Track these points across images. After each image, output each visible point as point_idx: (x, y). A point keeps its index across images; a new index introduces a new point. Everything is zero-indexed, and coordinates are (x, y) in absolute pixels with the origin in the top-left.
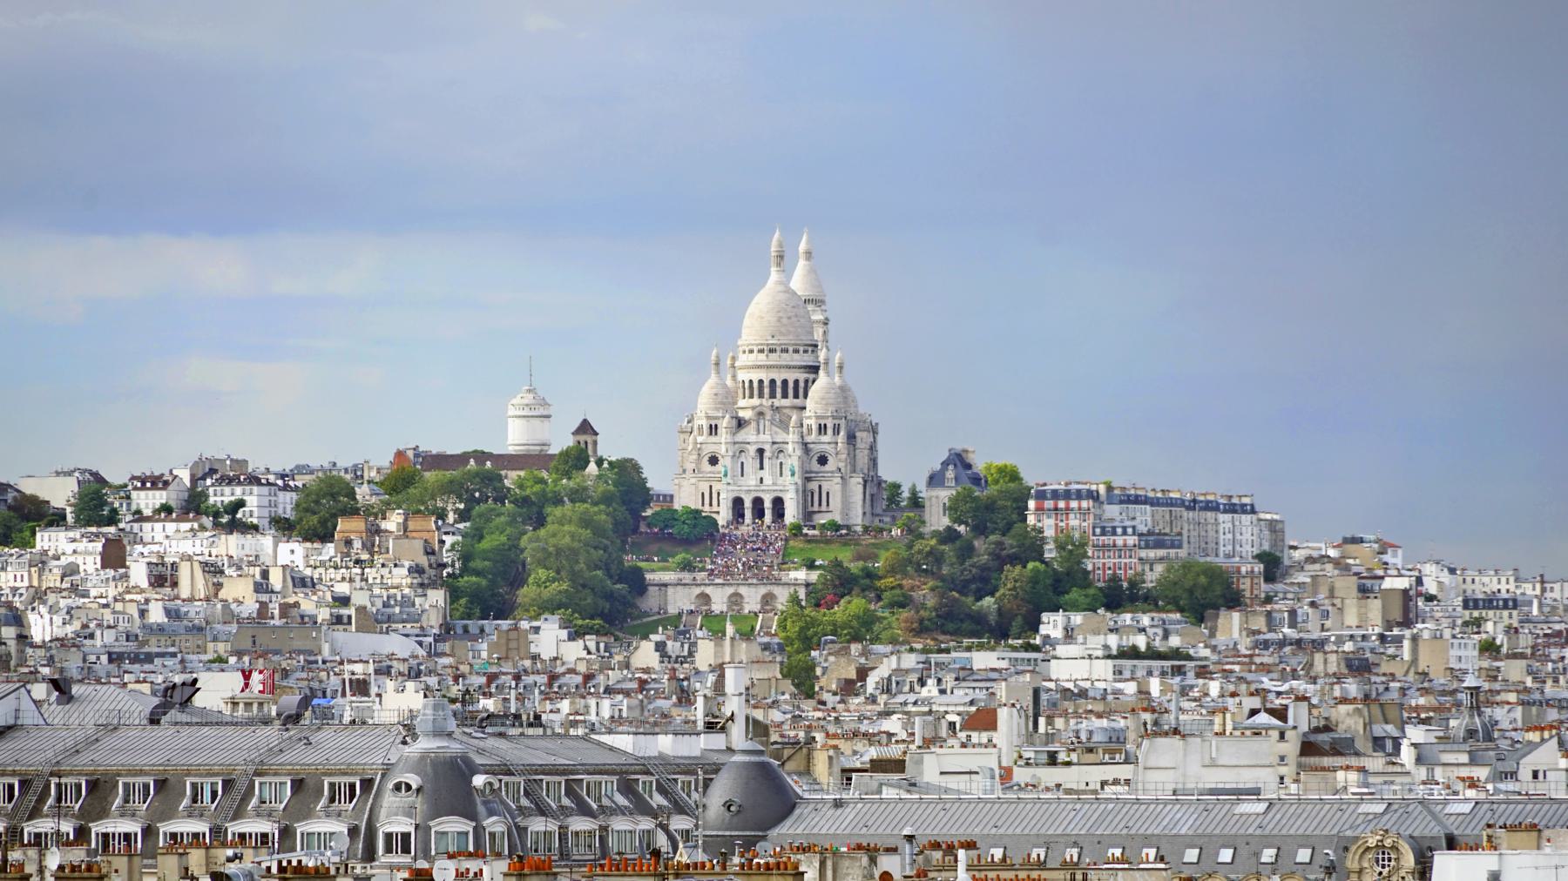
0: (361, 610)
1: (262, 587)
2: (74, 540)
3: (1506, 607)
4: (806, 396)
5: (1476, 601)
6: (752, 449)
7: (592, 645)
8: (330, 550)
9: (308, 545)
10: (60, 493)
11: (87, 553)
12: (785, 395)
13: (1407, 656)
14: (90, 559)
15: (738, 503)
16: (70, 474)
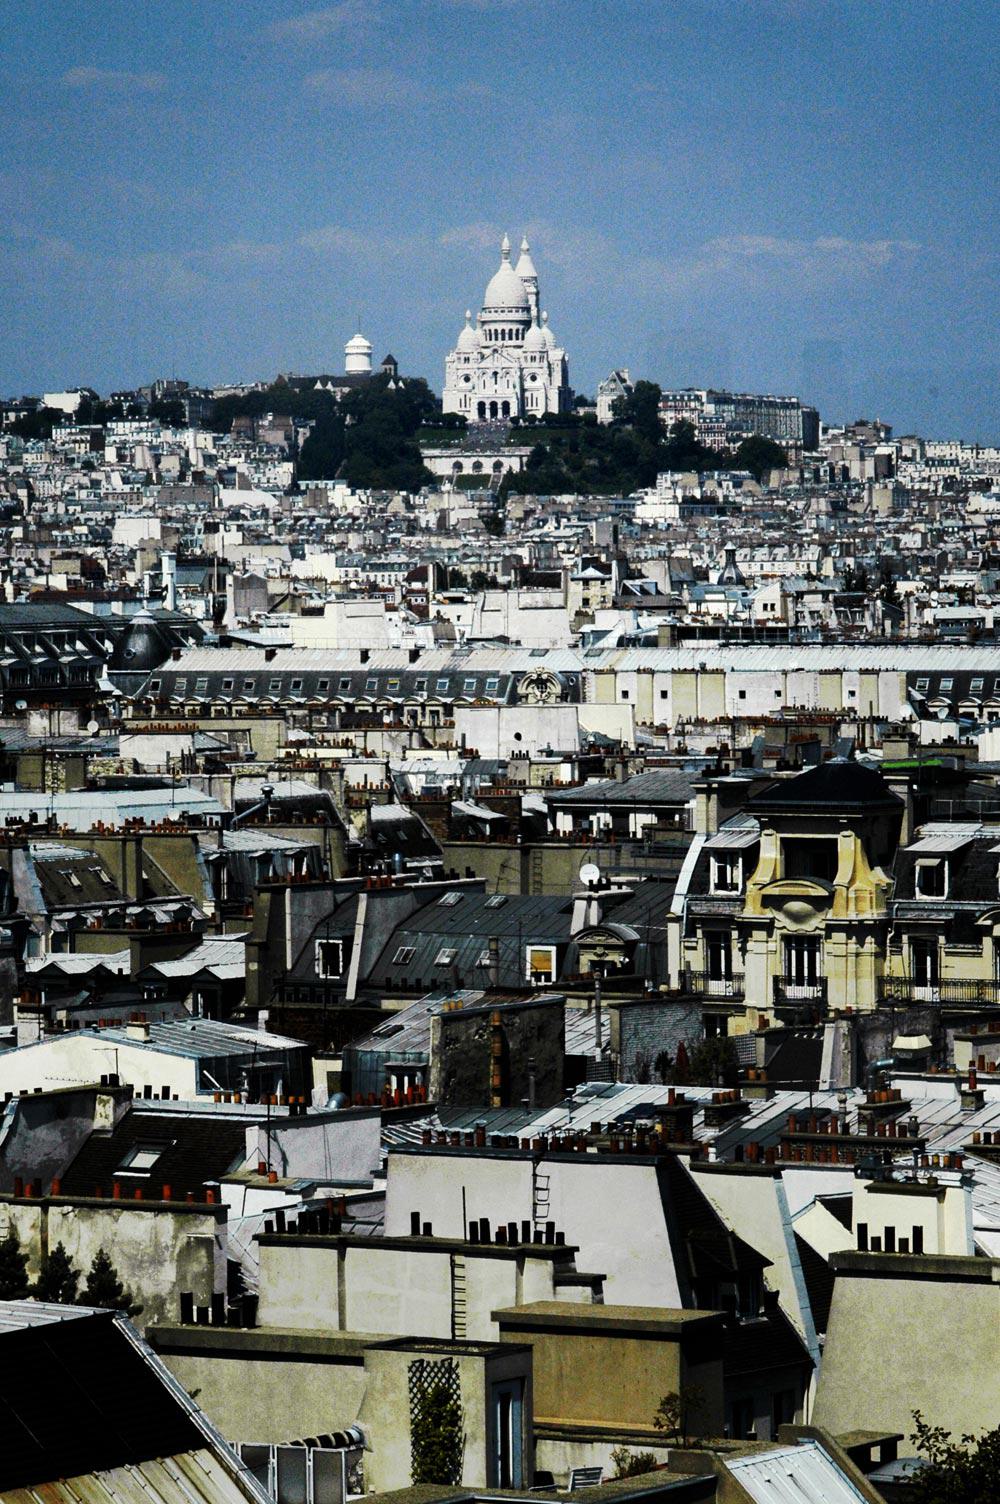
0: (242, 475)
1: (185, 464)
2: (71, 434)
3: (952, 464)
4: (523, 338)
5: (933, 460)
6: (490, 373)
7: (364, 498)
8: (228, 439)
9: (215, 435)
10: (69, 403)
11: (82, 441)
12: (511, 338)
13: (866, 500)
14: (83, 445)
15: (481, 406)
16: (76, 391)
